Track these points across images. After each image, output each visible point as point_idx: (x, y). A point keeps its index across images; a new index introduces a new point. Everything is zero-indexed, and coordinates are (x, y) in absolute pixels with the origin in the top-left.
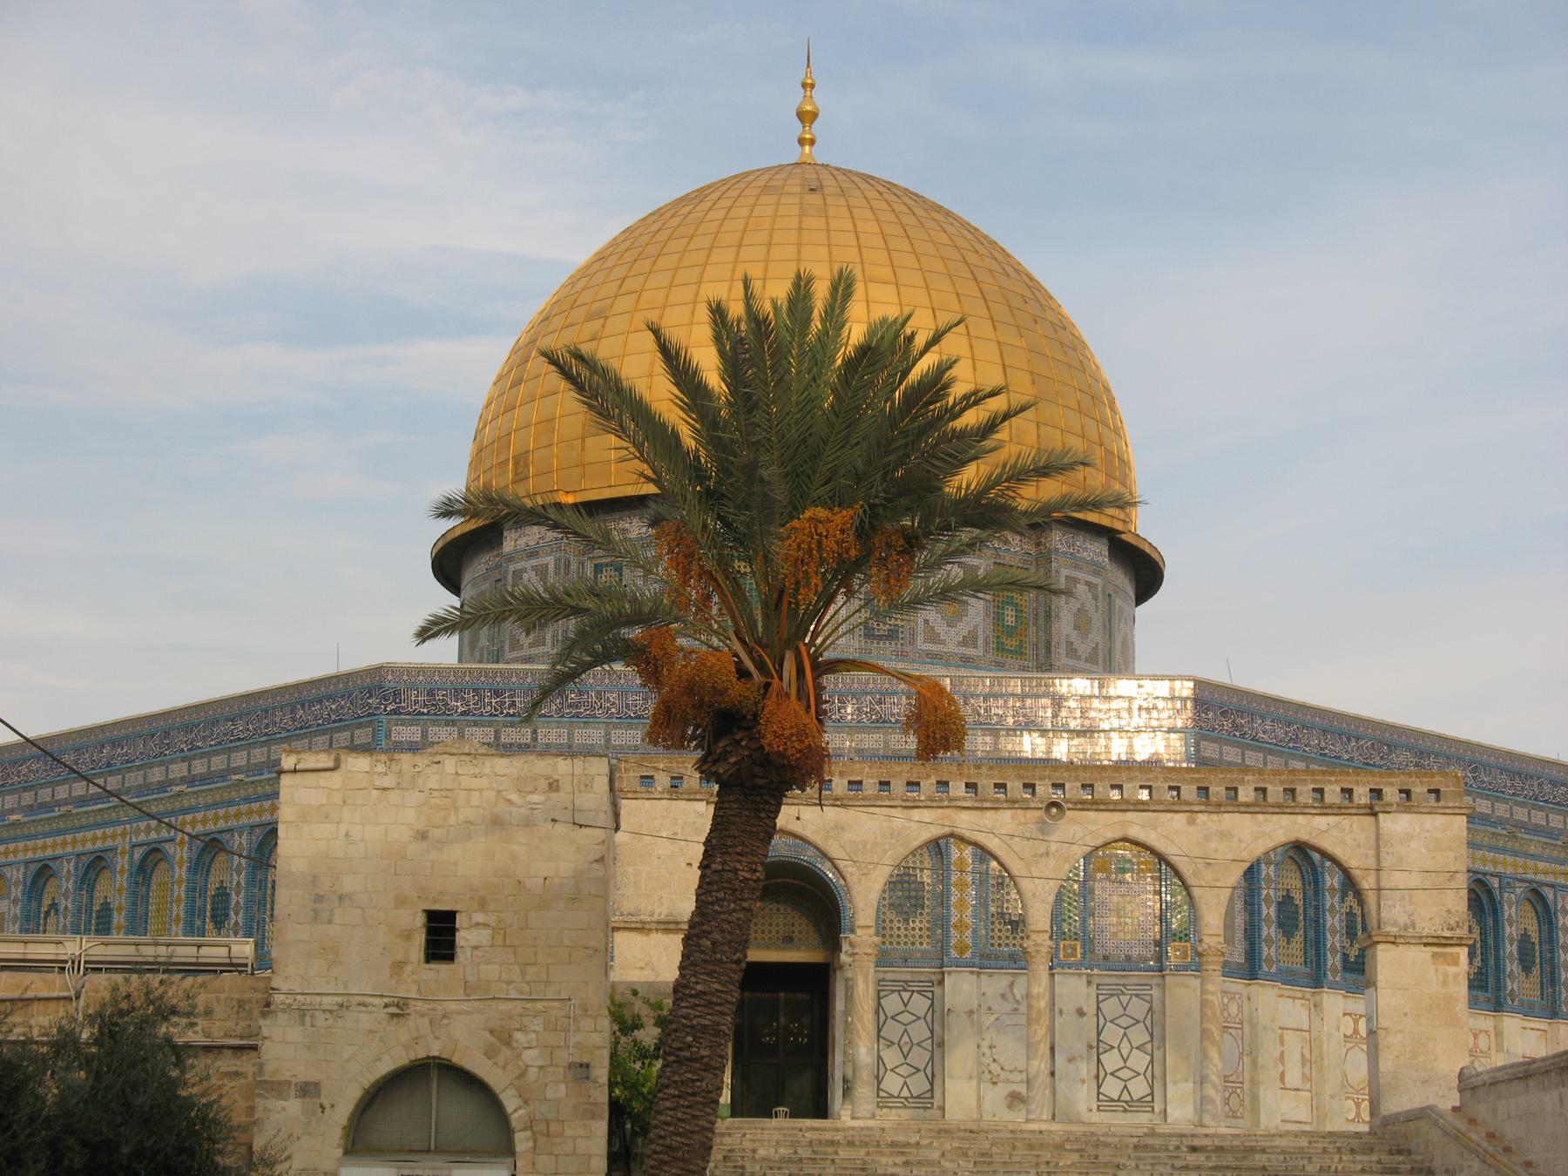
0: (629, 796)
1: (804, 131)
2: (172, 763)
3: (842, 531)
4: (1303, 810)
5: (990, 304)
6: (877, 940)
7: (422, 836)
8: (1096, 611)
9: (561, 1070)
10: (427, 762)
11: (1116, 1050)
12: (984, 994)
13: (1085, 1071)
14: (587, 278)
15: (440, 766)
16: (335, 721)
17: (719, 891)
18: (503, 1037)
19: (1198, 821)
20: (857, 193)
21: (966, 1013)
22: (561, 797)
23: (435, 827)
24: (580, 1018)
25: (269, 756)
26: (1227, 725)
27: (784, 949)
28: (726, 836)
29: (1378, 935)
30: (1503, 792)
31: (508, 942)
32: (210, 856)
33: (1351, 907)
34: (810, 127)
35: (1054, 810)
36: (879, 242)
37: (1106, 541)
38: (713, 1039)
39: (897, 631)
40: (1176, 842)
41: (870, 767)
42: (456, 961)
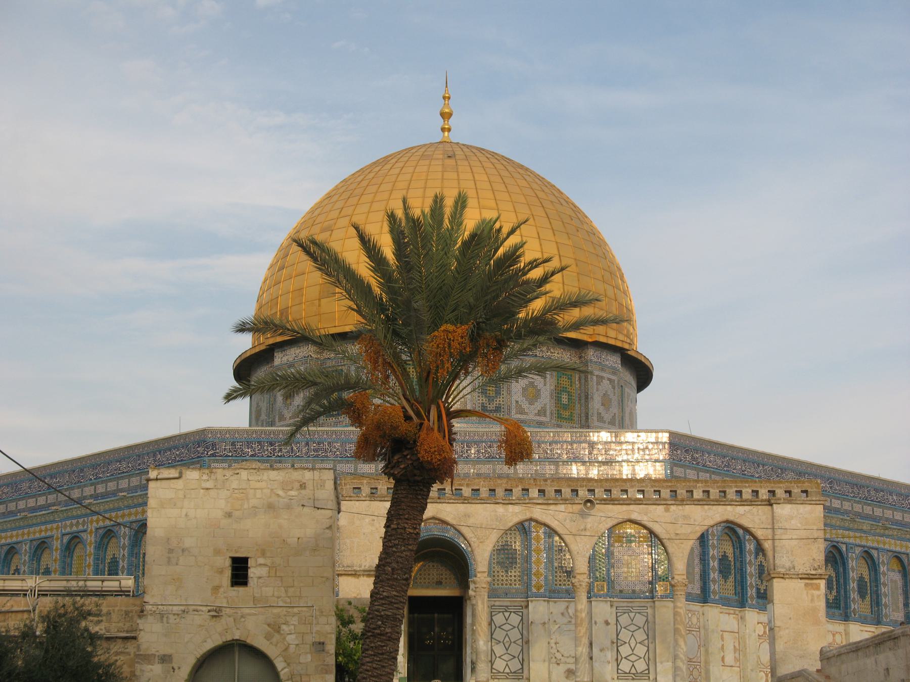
0: (347, 499)
3: (462, 337)
4: (731, 503)
5: (552, 221)
6: (489, 579)
7: (229, 515)
9: (308, 646)
10: (231, 473)
11: (627, 644)
12: (551, 613)
13: (610, 657)
15: (238, 475)
16: (178, 461)
18: (275, 628)
19: (671, 510)
20: (475, 158)
21: (541, 624)
24: (319, 617)
26: (689, 458)
27: (437, 589)
29: (773, 573)
30: (847, 495)
31: (278, 574)
32: (107, 540)
33: (761, 562)
34: (448, 121)
35: (589, 504)
37: (619, 355)
39: (500, 407)
41: (484, 481)
42: (249, 585)
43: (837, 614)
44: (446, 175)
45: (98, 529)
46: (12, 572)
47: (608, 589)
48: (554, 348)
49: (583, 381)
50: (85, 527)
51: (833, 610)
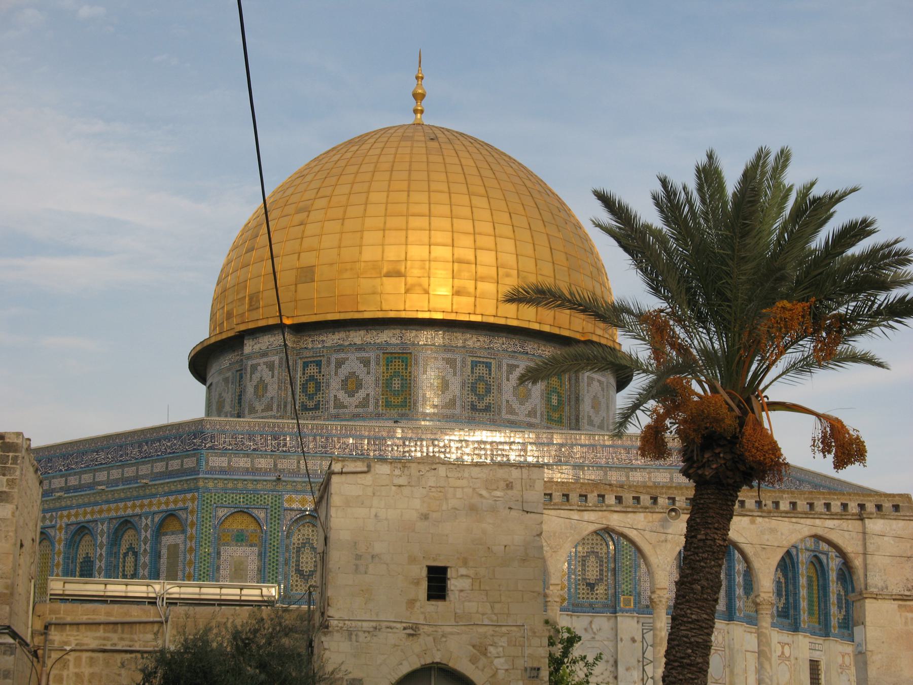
1: (417, 105)
2: (53, 478)
3: (803, 317)
4: (819, 516)
5: (541, 211)
7: (425, 517)
8: (603, 398)
9: (519, 672)
10: (427, 468)
13: (636, 676)
14: (293, 188)
16: (170, 453)
17: (704, 553)
18: (481, 650)
19: (757, 522)
20: (458, 142)
22: (515, 493)
23: (433, 511)
24: (531, 638)
25: (123, 474)
28: (707, 516)
29: (866, 593)
31: (482, 588)
33: (779, 578)
35: (674, 514)
36: (475, 172)
38: (704, 651)
39: (490, 407)
40: (744, 534)
42: (447, 598)
43: (846, 635)
44: (432, 158)
45: (69, 525)
46: (55, 574)
47: (635, 604)
48: (545, 346)
49: (573, 381)
50: (53, 523)
51: (843, 630)
